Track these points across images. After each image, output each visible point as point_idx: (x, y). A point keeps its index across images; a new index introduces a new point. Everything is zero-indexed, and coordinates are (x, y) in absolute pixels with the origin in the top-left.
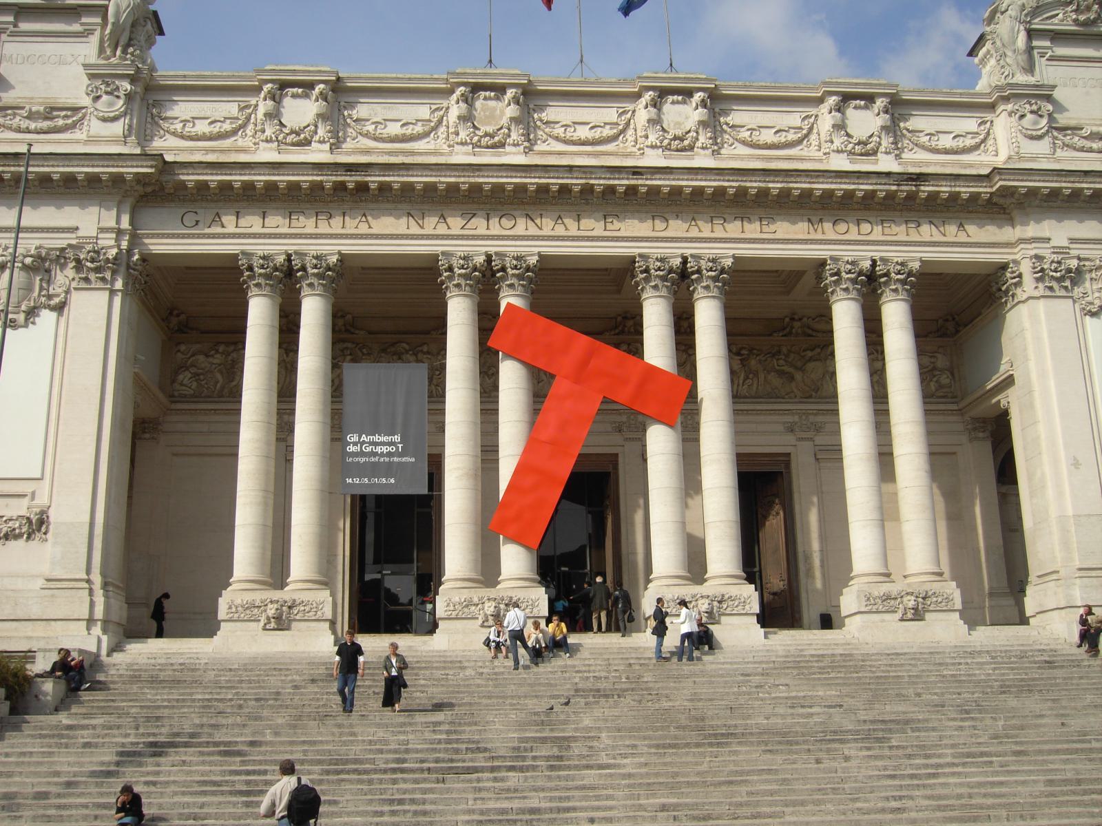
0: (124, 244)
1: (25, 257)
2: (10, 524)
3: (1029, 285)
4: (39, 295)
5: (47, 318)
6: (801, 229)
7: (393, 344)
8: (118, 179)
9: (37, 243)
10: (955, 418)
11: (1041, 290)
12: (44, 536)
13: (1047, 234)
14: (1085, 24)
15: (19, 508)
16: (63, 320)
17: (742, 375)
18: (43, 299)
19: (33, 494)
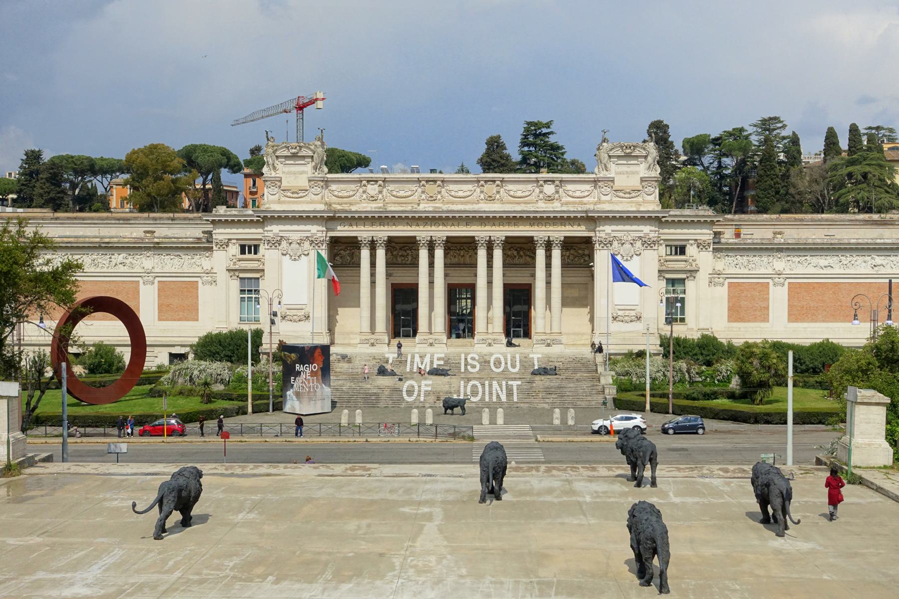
0: (324, 235)
3: (597, 245)
6: (528, 228)
7: (404, 247)
9: (300, 235)
10: (588, 272)
11: (600, 248)
15: (301, 313)
17: (517, 258)
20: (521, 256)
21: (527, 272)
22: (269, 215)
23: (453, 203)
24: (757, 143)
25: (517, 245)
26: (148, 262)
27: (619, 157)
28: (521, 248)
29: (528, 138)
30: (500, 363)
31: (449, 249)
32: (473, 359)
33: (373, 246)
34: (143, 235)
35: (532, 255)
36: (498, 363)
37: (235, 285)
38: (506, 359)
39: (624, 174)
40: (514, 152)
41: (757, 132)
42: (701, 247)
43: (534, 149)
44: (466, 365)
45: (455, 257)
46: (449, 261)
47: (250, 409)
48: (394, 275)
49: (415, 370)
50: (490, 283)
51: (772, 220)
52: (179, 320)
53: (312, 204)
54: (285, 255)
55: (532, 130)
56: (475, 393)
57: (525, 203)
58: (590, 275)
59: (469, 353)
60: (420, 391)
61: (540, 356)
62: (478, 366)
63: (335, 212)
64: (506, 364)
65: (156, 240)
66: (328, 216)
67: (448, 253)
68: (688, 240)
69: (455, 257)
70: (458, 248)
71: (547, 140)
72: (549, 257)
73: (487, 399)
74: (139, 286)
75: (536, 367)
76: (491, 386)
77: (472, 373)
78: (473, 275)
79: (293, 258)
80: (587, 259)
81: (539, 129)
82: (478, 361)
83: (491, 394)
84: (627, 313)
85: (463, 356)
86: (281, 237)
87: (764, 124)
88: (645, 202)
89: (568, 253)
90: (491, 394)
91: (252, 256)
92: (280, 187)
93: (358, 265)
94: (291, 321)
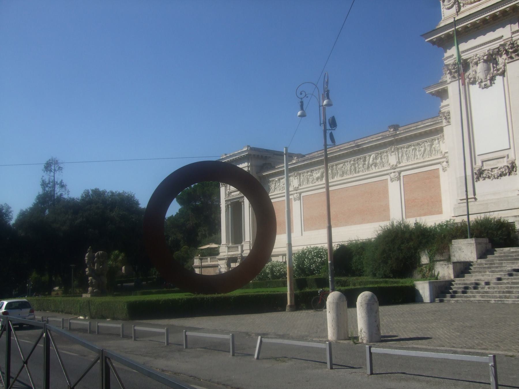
1: (484, 56)
2: (501, 170)
4: (494, 71)
5: (499, 79)
9: (488, 48)
12: (515, 173)
15: (504, 163)
16: (505, 78)
18: (495, 72)
19: (508, 156)
54: (474, 83)
74: (387, 184)
94: (489, 177)
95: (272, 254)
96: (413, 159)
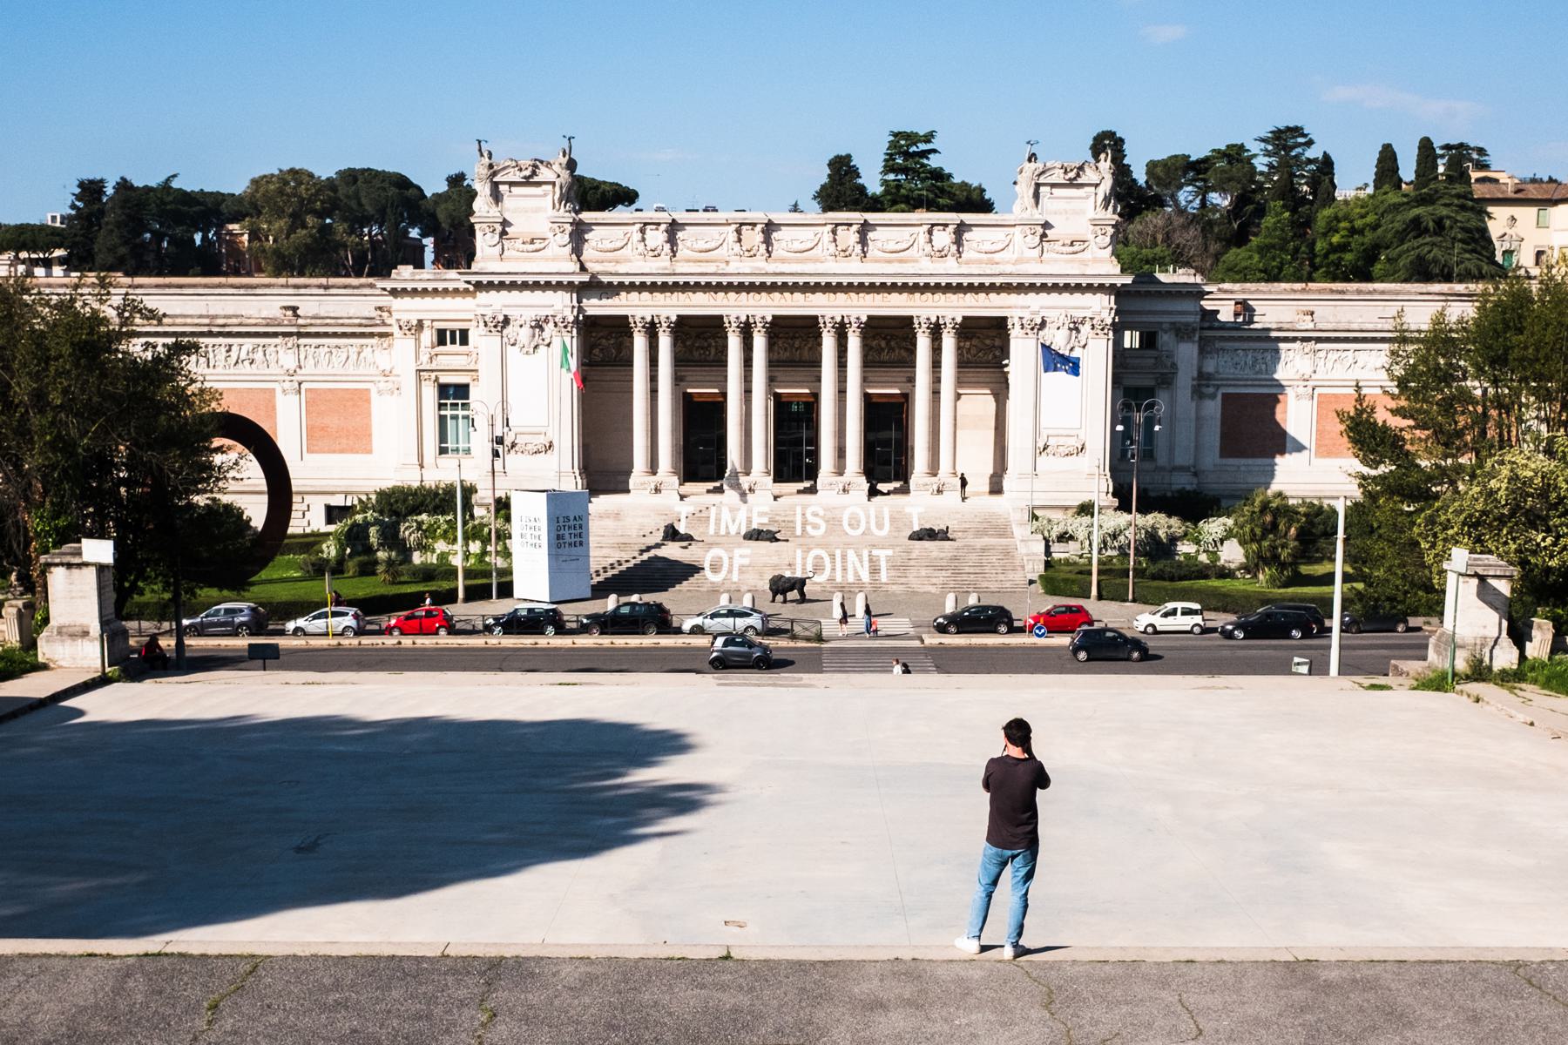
3: (1015, 333)
5: (542, 349)
7: (703, 333)
8: (571, 284)
13: (1028, 304)
14: (1070, 179)
20: (893, 350)
21: (899, 374)
22: (485, 279)
23: (783, 261)
24: (1266, 169)
25: (889, 331)
26: (284, 355)
27: (1053, 185)
28: (892, 336)
29: (894, 159)
30: (859, 522)
31: (776, 336)
32: (816, 515)
33: (652, 330)
34: (278, 313)
35: (910, 347)
36: (854, 524)
37: (430, 394)
38: (868, 517)
39: (1061, 213)
40: (872, 180)
41: (1266, 150)
42: (1181, 334)
43: (904, 177)
44: (804, 524)
45: (786, 349)
46: (776, 357)
47: (461, 594)
48: (688, 378)
49: (723, 532)
50: (842, 392)
51: (1294, 291)
52: (342, 451)
53: (557, 261)
55: (903, 146)
56: (818, 568)
57: (901, 261)
58: (1003, 380)
59: (809, 505)
60: (731, 565)
61: (921, 510)
62: (823, 526)
63: (593, 276)
64: (868, 522)
65: (300, 321)
66: (580, 282)
67: (775, 343)
68: (1161, 323)
69: (786, 349)
70: (791, 335)
71: (925, 161)
72: (936, 351)
73: (839, 579)
75: (916, 528)
76: (844, 557)
77: (813, 537)
78: (813, 379)
79: (525, 350)
80: (998, 353)
81: (915, 144)
82: (822, 518)
83: (845, 569)
84: (1062, 441)
85: (799, 511)
86: (506, 316)
87: (1278, 138)
88: (1096, 260)
89: (968, 343)
90: (845, 569)
91: (457, 348)
92: (503, 233)
93: (629, 363)
95: (290, 531)
96: (325, 366)
